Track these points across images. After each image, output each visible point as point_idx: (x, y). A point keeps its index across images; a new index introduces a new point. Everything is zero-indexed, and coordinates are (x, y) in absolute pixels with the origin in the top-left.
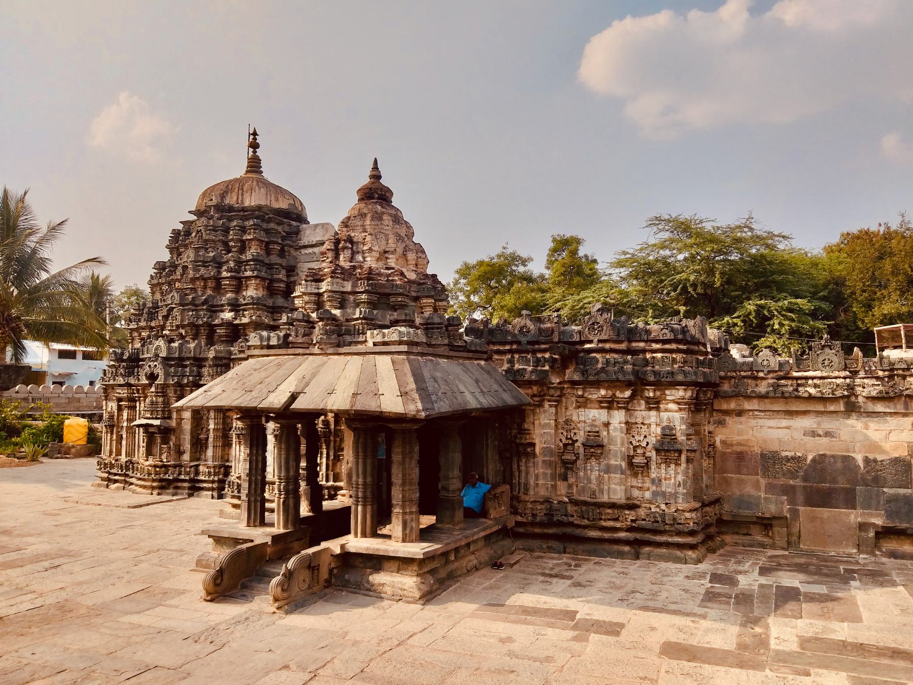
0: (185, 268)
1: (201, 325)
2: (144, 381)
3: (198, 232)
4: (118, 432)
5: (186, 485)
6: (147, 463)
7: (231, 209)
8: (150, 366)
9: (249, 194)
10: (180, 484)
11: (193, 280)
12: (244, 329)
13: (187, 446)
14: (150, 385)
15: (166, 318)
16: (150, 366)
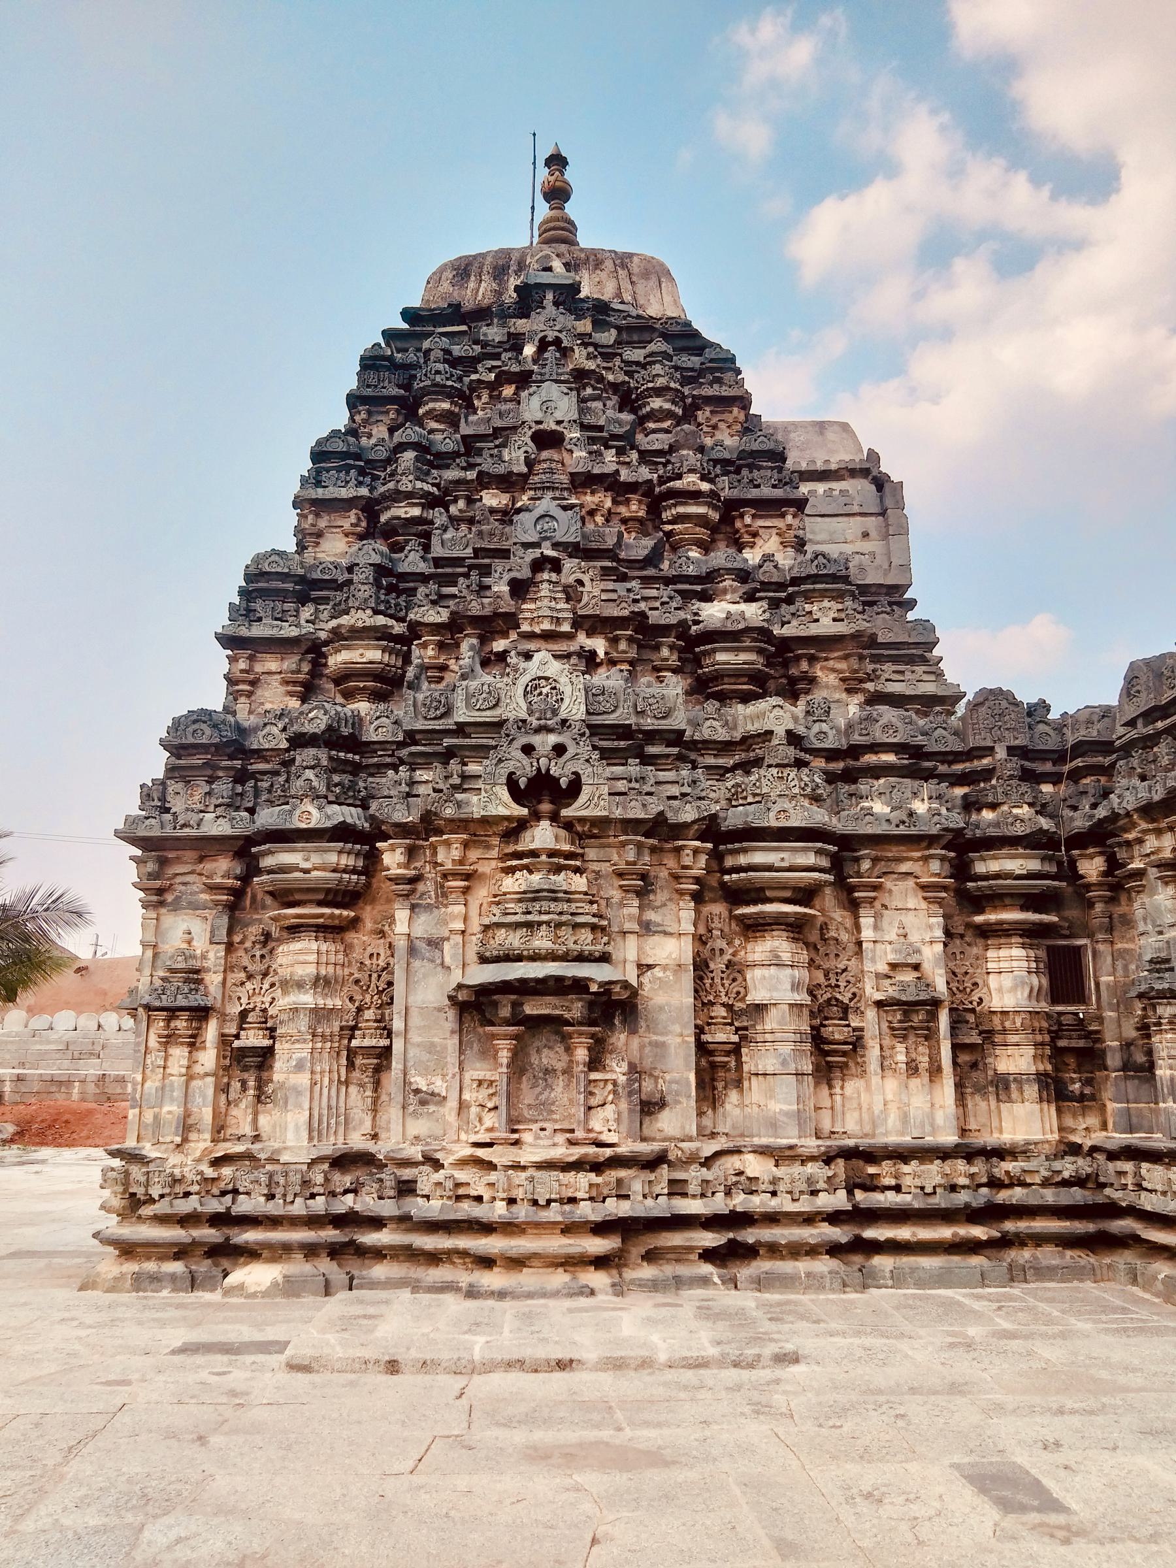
0: (547, 440)
1: (664, 630)
2: (504, 805)
3: (543, 346)
4: (224, 1041)
5: (710, 1239)
6: (527, 1156)
7: (600, 311)
8: (528, 749)
9: (653, 282)
10: (676, 1239)
11: (584, 481)
12: (812, 659)
13: (679, 1071)
14: (515, 829)
15: (520, 589)
16: (528, 749)
